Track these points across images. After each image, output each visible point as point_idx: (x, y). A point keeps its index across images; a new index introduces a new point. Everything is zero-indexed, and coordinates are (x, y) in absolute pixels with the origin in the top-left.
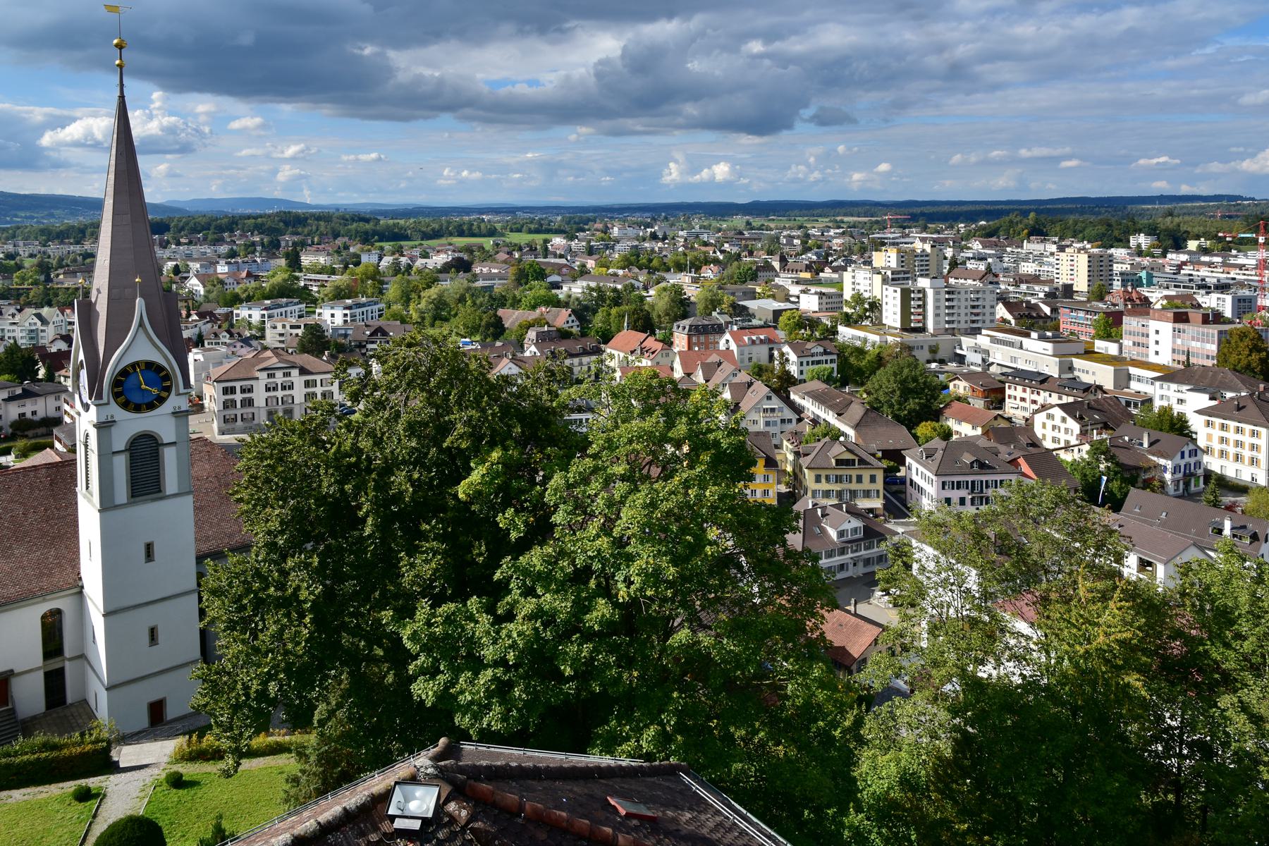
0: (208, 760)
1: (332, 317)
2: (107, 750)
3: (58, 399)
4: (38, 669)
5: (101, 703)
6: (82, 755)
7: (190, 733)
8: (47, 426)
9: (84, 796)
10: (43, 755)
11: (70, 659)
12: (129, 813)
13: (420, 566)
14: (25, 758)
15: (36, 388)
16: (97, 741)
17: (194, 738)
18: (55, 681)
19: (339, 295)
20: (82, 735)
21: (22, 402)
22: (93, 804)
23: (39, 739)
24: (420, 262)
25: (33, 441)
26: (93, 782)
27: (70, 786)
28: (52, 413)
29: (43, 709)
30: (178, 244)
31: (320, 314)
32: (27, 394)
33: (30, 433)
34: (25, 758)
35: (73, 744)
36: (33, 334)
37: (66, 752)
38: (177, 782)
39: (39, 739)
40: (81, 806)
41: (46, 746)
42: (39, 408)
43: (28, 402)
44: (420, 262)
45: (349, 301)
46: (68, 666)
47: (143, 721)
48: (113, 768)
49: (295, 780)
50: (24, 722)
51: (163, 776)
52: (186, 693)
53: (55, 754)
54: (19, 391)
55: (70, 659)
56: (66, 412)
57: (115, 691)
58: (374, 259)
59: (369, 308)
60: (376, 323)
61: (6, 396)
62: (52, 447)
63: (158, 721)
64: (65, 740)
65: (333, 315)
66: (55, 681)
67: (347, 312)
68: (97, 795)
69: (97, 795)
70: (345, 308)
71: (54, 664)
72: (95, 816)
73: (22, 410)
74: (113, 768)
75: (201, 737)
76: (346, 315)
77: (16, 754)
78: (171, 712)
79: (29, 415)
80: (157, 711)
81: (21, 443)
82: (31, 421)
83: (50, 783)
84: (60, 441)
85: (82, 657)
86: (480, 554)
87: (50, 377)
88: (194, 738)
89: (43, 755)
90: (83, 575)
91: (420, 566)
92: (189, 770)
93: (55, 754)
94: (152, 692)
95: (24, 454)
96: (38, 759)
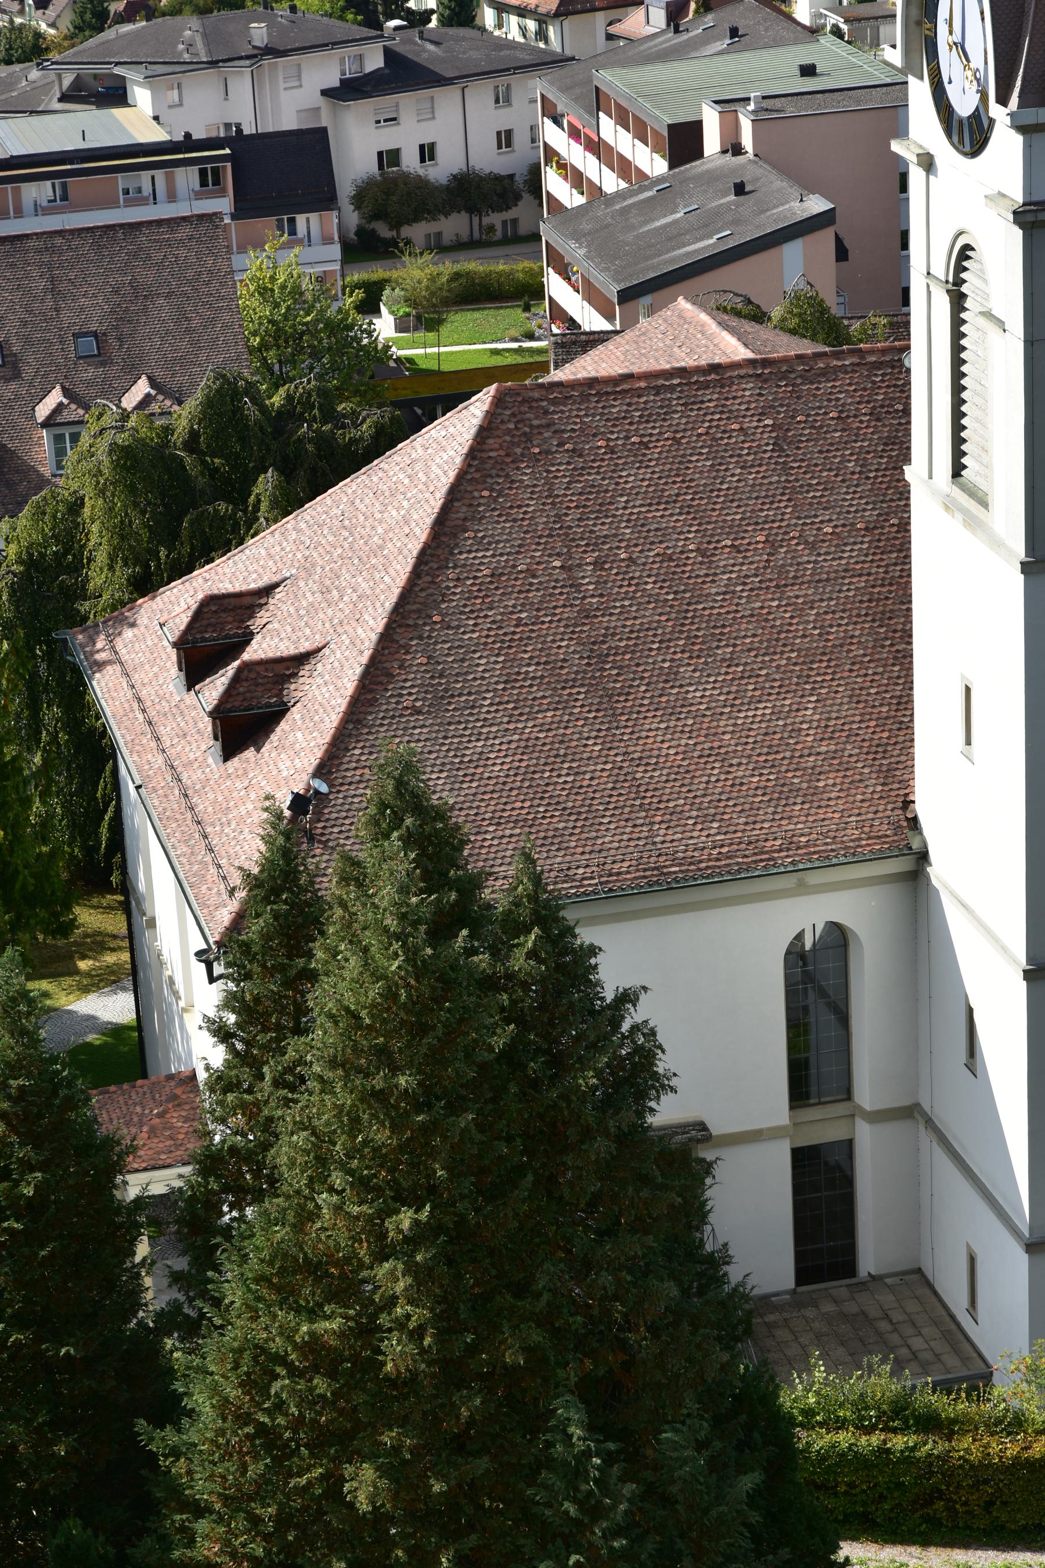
3: (503, 99)
8: (472, 210)
10: (899, 1442)
11: (877, 1117)
14: (844, 1438)
15: (427, 53)
18: (823, 1185)
21: (385, 103)
25: (448, 267)
28: (487, 159)
29: (790, 1283)
32: (402, 75)
33: (418, 232)
34: (844, 1438)
41: (900, 1414)
42: (446, 132)
43: (407, 103)
46: (865, 1135)
53: (932, 1446)
54: (374, 61)
55: (877, 1117)
56: (551, 154)
62: (531, 292)
66: (823, 1185)
71: (823, 1128)
73: (388, 139)
79: (410, 161)
81: (417, 271)
82: (422, 184)
83: (925, 1542)
84: (564, 272)
89: (899, 1442)
90: (922, 808)
93: (932, 1446)
95: (423, 318)
96: (883, 1451)
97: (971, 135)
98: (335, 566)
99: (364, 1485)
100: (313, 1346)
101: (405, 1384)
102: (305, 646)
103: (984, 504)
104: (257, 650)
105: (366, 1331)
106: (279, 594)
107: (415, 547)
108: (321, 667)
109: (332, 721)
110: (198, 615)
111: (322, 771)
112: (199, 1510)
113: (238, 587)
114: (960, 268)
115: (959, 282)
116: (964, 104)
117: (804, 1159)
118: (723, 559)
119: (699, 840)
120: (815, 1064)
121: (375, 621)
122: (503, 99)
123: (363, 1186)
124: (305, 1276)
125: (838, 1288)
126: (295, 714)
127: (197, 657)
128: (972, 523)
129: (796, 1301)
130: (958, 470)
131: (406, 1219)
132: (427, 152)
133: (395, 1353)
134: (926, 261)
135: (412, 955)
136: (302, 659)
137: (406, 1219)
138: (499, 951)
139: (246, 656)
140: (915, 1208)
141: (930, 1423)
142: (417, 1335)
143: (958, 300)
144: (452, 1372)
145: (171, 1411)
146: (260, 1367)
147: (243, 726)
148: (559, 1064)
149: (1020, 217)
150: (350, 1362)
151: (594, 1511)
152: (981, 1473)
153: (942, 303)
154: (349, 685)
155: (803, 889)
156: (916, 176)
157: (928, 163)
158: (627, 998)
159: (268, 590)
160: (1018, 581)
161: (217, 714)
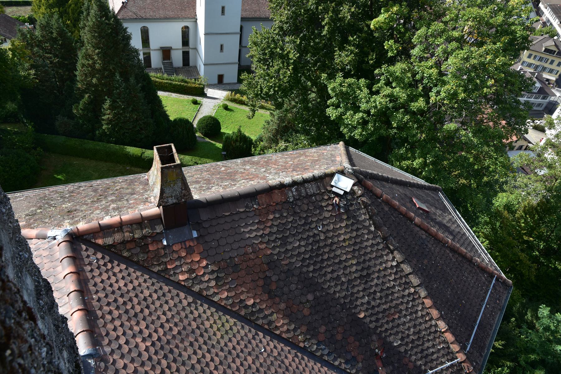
0: (237, 103)
2: (203, 89)
4: (180, 49)
5: (202, 69)
6: (195, 88)
7: (232, 91)
9: (195, 103)
10: (182, 84)
12: (210, 114)
13: (344, 57)
16: (200, 84)
17: (233, 93)
18: (186, 55)
20: (195, 80)
22: (198, 106)
23: (181, 77)
26: (198, 99)
27: (191, 98)
35: (192, 83)
37: (189, 85)
38: (226, 108)
39: (181, 77)
40: (194, 106)
41: (183, 81)
47: (216, 81)
48: (204, 95)
49: (268, 123)
50: (175, 68)
51: (221, 104)
52: (231, 74)
53: (186, 84)
57: (206, 66)
63: (220, 82)
64: (188, 80)
68: (199, 104)
69: (199, 104)
71: (186, 49)
72: (198, 111)
74: (204, 95)
75: (236, 94)
77: (173, 80)
78: (225, 80)
80: (221, 78)
85: (196, 49)
86: (372, 59)
88: (233, 93)
89: (182, 84)
91: (344, 57)
92: (231, 105)
93: (186, 84)
94: (220, 70)
99: (94, 81)
100: (88, 64)
101: (100, 70)
105: (94, 63)
112: (78, 81)
117: (183, 52)
119: (171, 14)
120: (185, 42)
123: (93, 47)
124: (87, 56)
125: (187, 67)
129: (182, 68)
131: (97, 51)
133: (97, 66)
135: (97, 20)
137: (97, 51)
138: (109, 21)
140: (196, 60)
141: (186, 82)
142: (100, 64)
144: (104, 69)
145: (76, 70)
146: (83, 65)
148: (117, 34)
150: (92, 66)
151: (121, 86)
152: (191, 88)
155: (183, 21)
158: (126, 28)
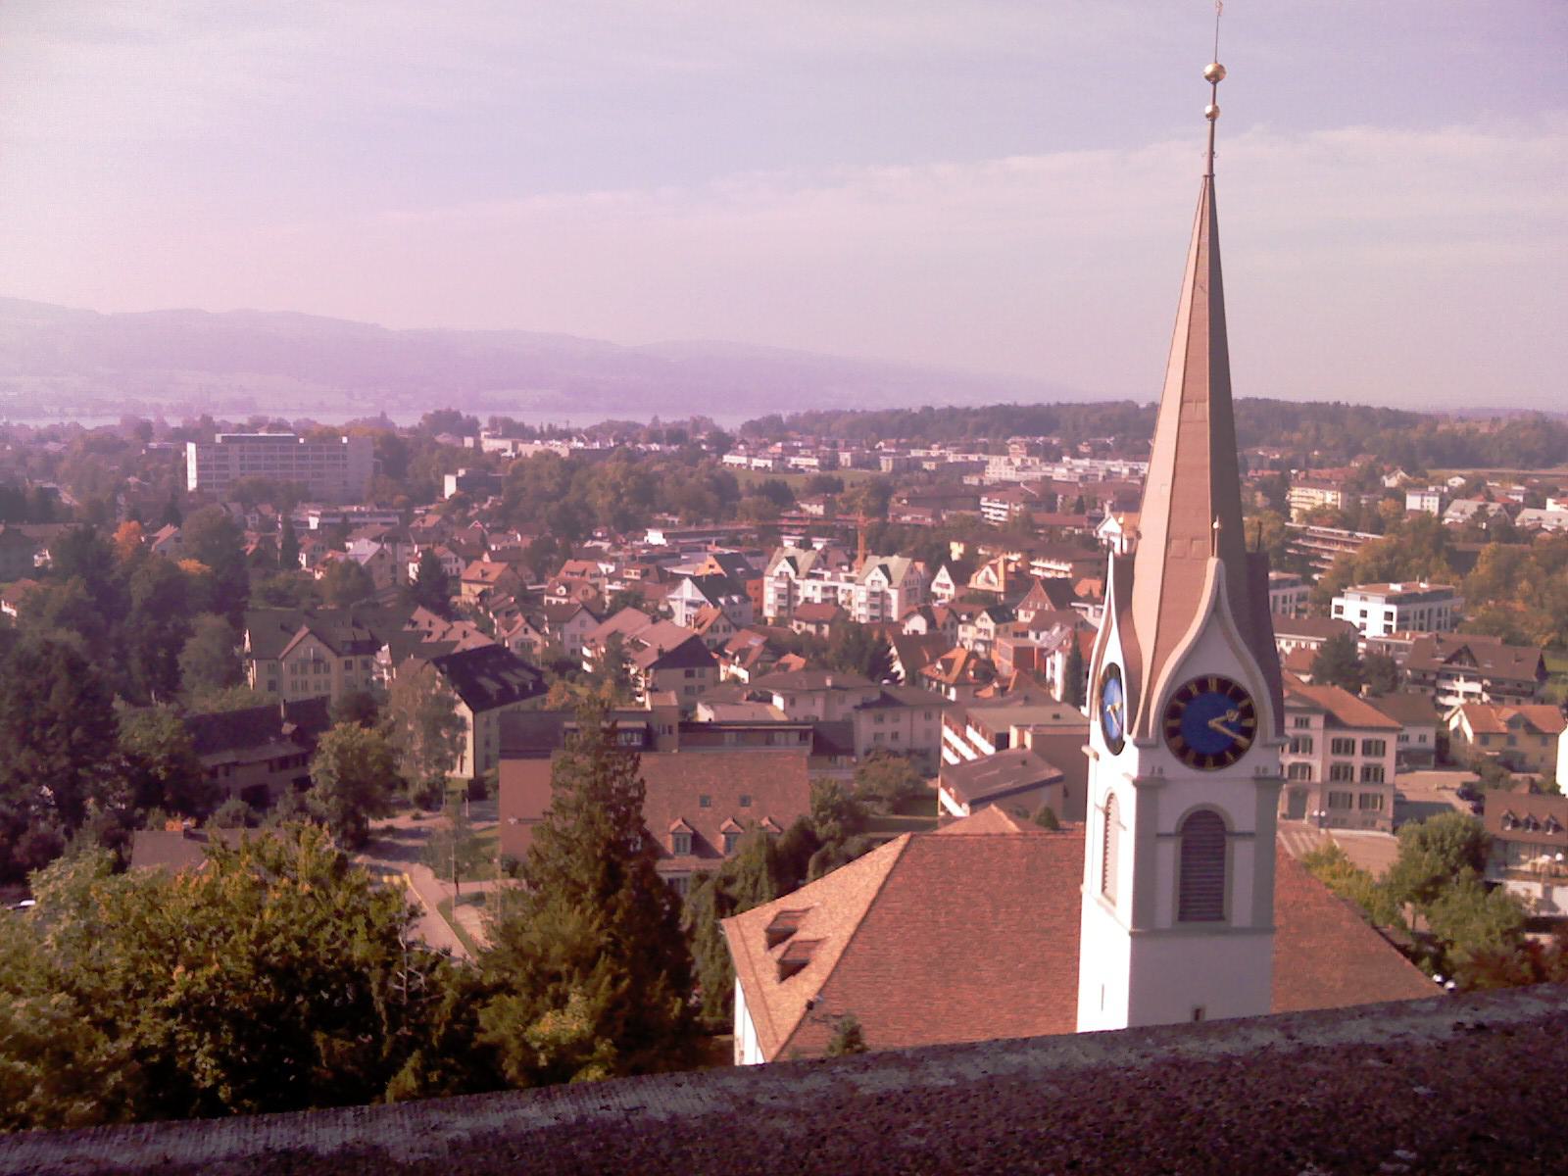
1: (1368, 614)
3: (928, 716)
19: (1375, 576)
21: (876, 711)
24: (1528, 515)
28: (921, 743)
30: (1077, 455)
31: (1340, 609)
36: (879, 599)
43: (888, 714)
44: (1528, 515)
45: (1396, 588)
54: (876, 697)
58: (1432, 504)
59: (1435, 606)
60: (1457, 638)
61: (858, 702)
65: (1364, 614)
67: (1393, 609)
70: (1389, 601)
76: (1389, 616)
87: (914, 678)
97: (1116, 746)
98: (836, 902)
102: (819, 936)
103: (1114, 903)
104: (800, 935)
106: (811, 912)
107: (870, 898)
108: (827, 946)
109: (827, 971)
110: (776, 918)
111: (820, 992)
113: (795, 908)
114: (1109, 802)
115: (1108, 808)
116: (1115, 733)
118: (1001, 917)
121: (850, 929)
122: (928, 716)
126: (812, 966)
127: (776, 936)
128: (1110, 912)
130: (1104, 888)
132: (895, 736)
134: (1095, 797)
136: (817, 941)
139: (796, 937)
143: (1107, 815)
147: (790, 969)
149: (1137, 783)
153: (1102, 817)
154: (837, 954)
156: (1092, 761)
157: (1097, 757)
159: (806, 911)
160: (1128, 939)
161: (781, 962)
